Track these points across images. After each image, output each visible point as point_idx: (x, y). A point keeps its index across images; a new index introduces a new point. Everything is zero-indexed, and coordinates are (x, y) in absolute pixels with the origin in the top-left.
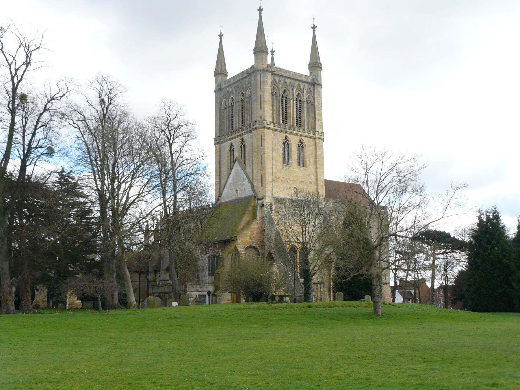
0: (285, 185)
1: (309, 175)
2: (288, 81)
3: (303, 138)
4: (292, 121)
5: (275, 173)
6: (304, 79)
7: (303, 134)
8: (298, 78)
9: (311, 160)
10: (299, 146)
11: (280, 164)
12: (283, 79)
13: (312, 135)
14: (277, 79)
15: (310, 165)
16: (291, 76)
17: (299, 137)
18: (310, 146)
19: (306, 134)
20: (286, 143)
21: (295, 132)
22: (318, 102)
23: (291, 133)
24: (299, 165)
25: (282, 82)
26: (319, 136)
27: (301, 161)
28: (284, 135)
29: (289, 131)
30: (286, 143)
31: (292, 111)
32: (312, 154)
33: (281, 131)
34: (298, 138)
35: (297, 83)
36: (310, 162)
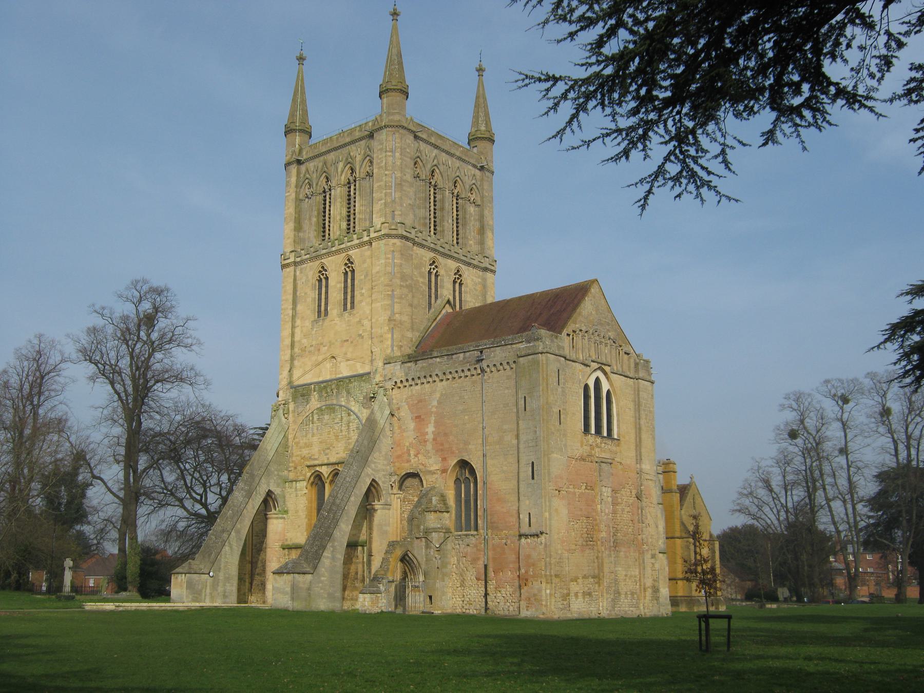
0: (314, 358)
1: (360, 321)
2: (331, 157)
3: (350, 253)
4: (337, 226)
5: (299, 341)
6: (357, 134)
7: (349, 244)
8: (348, 140)
9: (363, 291)
10: (346, 274)
11: (308, 324)
12: (322, 158)
13: (366, 239)
14: (311, 165)
15: (361, 301)
16: (336, 145)
17: (344, 254)
18: (364, 262)
19: (356, 242)
20: (323, 279)
21: (334, 249)
22: (378, 164)
23: (329, 254)
24: (345, 309)
25: (320, 165)
26: (376, 235)
27: (349, 302)
28: (316, 264)
29: (324, 251)
30: (323, 279)
31: (337, 210)
32: (366, 276)
33: (311, 259)
34: (340, 259)
35: (345, 151)
36: (362, 295)
